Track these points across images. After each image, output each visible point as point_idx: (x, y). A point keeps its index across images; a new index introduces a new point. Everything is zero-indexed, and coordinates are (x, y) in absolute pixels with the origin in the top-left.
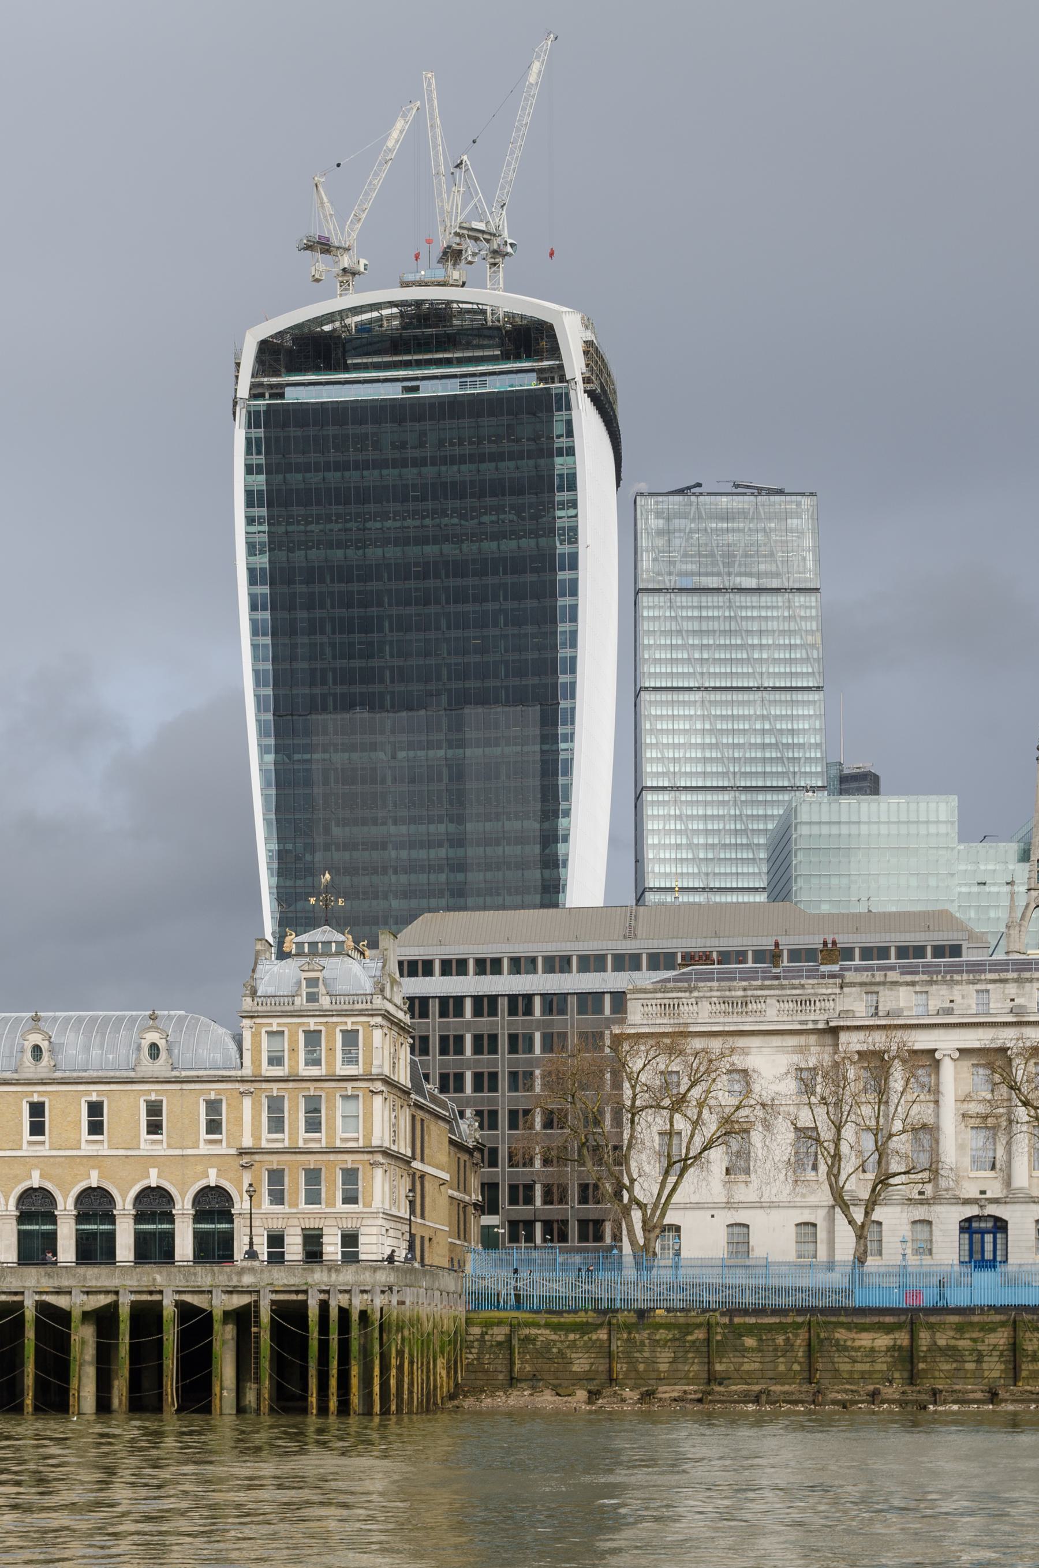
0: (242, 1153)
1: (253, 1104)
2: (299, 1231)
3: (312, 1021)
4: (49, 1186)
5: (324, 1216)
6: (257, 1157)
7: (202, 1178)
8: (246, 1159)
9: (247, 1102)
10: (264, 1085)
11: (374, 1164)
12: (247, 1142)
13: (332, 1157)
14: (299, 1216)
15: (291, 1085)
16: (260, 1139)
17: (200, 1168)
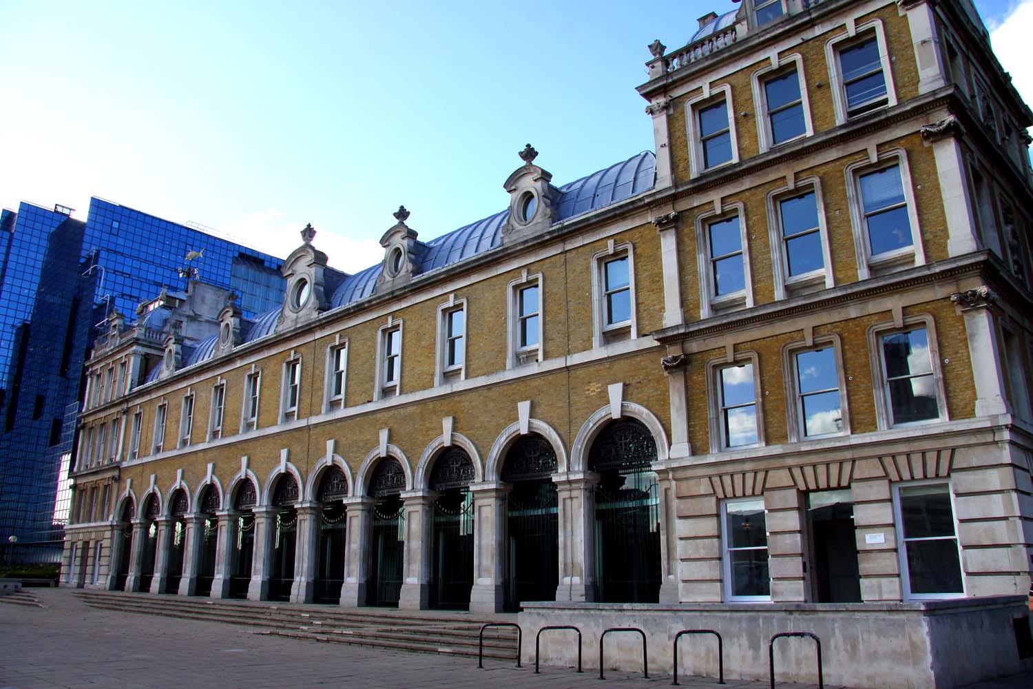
0: (666, 340)
1: (679, 243)
2: (792, 498)
3: (772, 54)
4: (397, 452)
5: (849, 455)
6: (694, 346)
7: (599, 407)
8: (674, 351)
9: (668, 244)
10: (697, 201)
11: (969, 301)
12: (672, 316)
13: (853, 311)
14: (790, 461)
15: (747, 183)
16: (697, 306)
17: (594, 388)
